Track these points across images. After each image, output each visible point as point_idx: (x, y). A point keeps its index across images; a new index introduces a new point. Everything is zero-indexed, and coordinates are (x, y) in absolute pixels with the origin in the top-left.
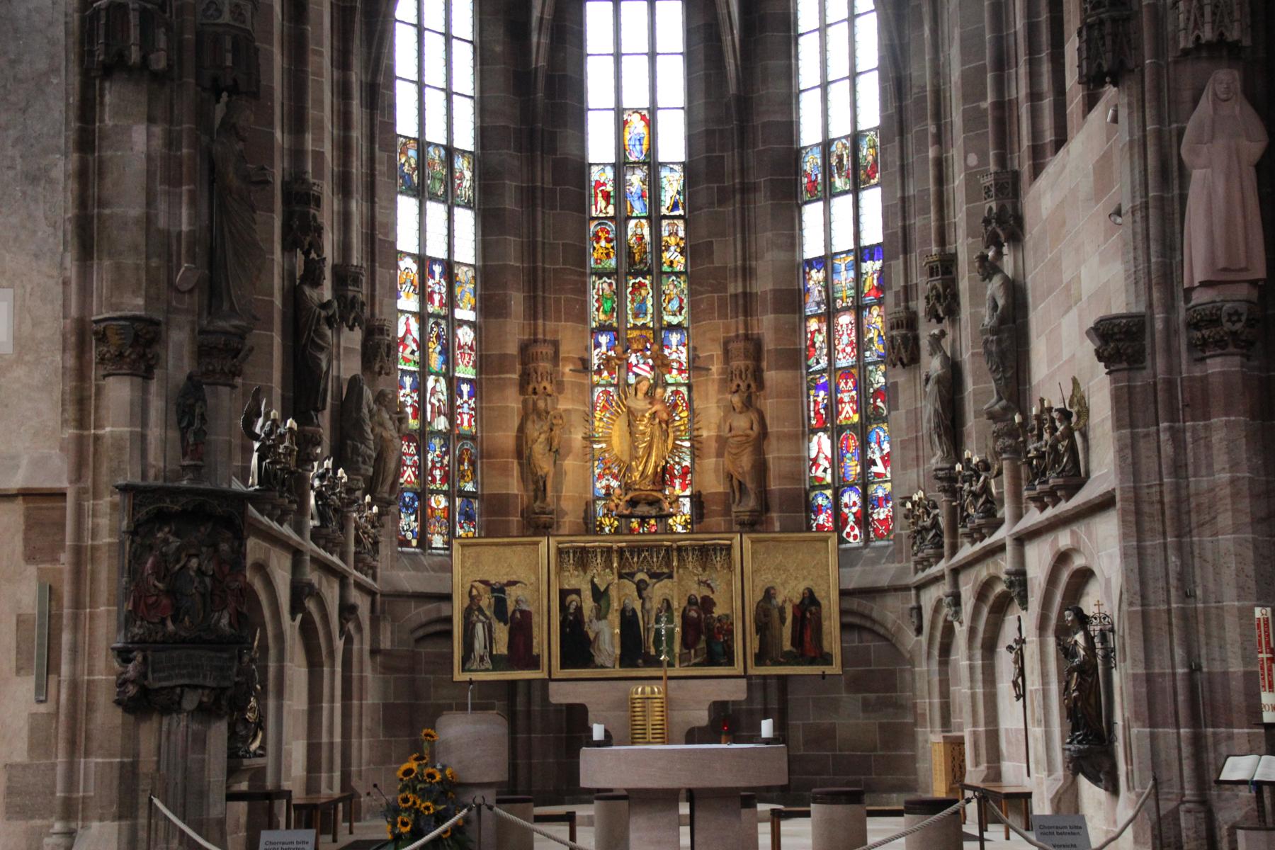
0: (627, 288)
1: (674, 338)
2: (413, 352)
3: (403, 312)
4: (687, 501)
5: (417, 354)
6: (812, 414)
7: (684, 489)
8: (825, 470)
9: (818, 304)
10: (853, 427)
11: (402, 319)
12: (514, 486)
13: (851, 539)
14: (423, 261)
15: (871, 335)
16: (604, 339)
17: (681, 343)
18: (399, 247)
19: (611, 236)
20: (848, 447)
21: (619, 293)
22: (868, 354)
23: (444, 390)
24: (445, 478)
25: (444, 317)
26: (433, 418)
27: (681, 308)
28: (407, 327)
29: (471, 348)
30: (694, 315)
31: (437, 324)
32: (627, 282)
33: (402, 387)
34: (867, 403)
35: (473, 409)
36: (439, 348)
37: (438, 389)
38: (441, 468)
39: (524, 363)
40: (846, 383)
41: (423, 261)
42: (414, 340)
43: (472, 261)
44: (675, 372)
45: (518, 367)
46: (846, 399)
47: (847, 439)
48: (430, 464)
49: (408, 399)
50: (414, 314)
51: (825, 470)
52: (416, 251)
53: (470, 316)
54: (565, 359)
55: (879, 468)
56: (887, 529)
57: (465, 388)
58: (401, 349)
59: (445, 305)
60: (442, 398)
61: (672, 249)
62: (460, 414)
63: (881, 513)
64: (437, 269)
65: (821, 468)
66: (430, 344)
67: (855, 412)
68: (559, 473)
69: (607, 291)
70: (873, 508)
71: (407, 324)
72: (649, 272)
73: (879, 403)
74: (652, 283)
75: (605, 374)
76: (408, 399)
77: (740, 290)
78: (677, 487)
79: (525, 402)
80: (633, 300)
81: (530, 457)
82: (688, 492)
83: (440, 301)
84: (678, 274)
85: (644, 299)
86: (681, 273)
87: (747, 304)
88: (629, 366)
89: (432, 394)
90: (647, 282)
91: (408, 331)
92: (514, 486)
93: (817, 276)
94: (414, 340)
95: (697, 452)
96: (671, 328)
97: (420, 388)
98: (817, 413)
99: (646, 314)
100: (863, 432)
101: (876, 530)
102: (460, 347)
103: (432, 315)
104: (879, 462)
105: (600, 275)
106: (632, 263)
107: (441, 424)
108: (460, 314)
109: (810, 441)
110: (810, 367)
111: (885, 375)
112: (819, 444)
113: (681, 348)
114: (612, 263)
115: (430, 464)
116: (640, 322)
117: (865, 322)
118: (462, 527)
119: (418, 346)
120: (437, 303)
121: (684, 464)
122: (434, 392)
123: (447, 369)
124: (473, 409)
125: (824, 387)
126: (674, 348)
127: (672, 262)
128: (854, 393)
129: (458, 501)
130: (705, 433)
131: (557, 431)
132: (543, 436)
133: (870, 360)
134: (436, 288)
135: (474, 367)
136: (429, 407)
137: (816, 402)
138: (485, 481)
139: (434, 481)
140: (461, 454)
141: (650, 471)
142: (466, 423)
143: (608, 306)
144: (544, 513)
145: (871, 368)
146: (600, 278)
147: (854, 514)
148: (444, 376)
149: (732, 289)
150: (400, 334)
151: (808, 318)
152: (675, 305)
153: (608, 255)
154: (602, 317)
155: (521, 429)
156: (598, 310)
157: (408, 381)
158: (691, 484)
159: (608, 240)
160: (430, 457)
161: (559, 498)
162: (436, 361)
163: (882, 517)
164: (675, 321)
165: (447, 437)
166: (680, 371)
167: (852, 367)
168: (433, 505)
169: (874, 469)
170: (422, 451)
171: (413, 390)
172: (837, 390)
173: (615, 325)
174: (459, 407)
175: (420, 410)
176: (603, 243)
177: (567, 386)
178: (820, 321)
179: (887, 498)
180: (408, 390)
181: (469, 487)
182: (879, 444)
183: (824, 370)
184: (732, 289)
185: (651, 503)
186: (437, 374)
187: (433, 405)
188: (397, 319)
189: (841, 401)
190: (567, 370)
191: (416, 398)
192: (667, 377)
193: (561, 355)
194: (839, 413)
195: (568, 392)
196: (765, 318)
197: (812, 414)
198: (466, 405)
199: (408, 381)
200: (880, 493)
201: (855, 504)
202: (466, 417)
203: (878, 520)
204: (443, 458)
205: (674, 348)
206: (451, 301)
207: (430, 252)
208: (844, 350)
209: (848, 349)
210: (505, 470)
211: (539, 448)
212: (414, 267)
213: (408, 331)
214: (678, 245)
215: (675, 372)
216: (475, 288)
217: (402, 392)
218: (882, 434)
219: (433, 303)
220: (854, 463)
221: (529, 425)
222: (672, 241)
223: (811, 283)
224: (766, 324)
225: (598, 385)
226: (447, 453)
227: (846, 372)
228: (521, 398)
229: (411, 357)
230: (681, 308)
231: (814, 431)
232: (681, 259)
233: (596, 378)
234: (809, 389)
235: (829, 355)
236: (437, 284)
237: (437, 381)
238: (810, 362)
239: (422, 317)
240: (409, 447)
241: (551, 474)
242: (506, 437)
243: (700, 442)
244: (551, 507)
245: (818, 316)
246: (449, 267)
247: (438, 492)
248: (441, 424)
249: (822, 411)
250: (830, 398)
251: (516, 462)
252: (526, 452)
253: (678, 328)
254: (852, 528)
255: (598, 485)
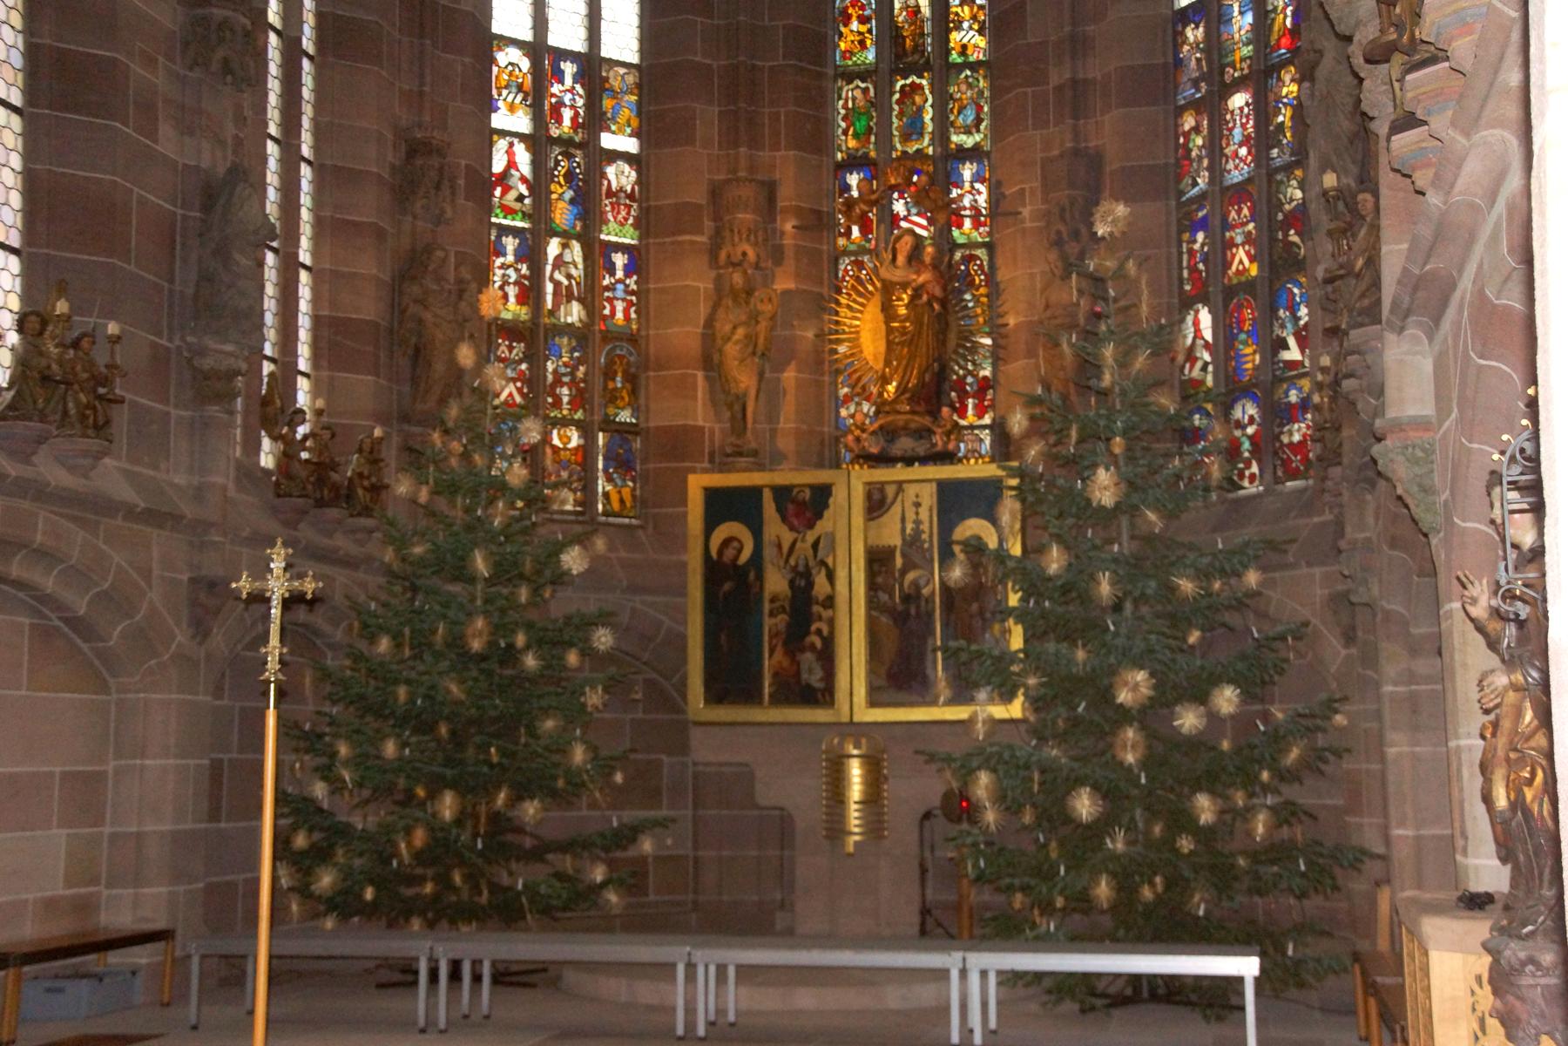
0: (892, 93)
1: (967, 172)
2: (520, 198)
3: (503, 133)
4: (986, 436)
5: (527, 201)
6: (1185, 274)
7: (980, 416)
8: (1204, 368)
9: (1195, 83)
10: (1250, 286)
11: (501, 145)
12: (700, 414)
13: (1246, 483)
14: (538, 49)
15: (1281, 119)
16: (853, 179)
17: (977, 178)
18: (497, 28)
19: (868, 12)
20: (1241, 322)
21: (879, 104)
22: (1275, 152)
23: (579, 260)
24: (578, 400)
25: (580, 146)
26: (556, 305)
27: (979, 121)
28: (511, 158)
29: (631, 196)
30: (997, 133)
31: (569, 156)
32: (892, 84)
33: (501, 253)
34: (1273, 239)
35: (633, 293)
36: (569, 194)
37: (567, 258)
38: (569, 385)
39: (717, 218)
40: (1239, 212)
41: (538, 49)
42: (523, 179)
43: (634, 58)
44: (968, 223)
45: (708, 224)
46: (1239, 240)
47: (1240, 307)
48: (550, 378)
49: (511, 272)
50: (522, 137)
51: (1204, 368)
52: (527, 35)
53: (630, 145)
54: (785, 211)
55: (1293, 354)
56: (1306, 460)
57: (620, 260)
58: (498, 192)
59: (583, 126)
60: (573, 272)
61: (966, 25)
62: (610, 300)
63: (1297, 432)
64: (569, 69)
65: (1199, 365)
66: (553, 187)
67: (1252, 259)
68: (770, 392)
69: (861, 102)
70: (1282, 425)
71: (510, 152)
72: (927, 66)
73: (1294, 237)
74: (932, 85)
75: (856, 231)
76: (511, 272)
77: (1068, 76)
78: (970, 412)
79: (718, 280)
80: (901, 113)
81: (721, 363)
82: (987, 420)
83: (574, 119)
84: (974, 66)
85: (920, 110)
86: (979, 63)
87: (1077, 98)
88: (895, 219)
89: (556, 266)
90: (924, 82)
91: (512, 164)
92: (700, 414)
93: (1194, 34)
94: (523, 179)
95: (1002, 353)
96: (964, 154)
97: (532, 254)
98: (1193, 269)
99: (921, 135)
100: (1268, 293)
101: (1286, 463)
102: (610, 193)
103: (559, 141)
104: (1292, 341)
105: (849, 76)
106: (900, 54)
107: (574, 313)
108: (608, 141)
109: (1183, 320)
110: (1182, 193)
111: (1301, 187)
112: (1196, 323)
113: (977, 185)
114: (870, 56)
115: (550, 378)
116: (912, 148)
117: (1271, 97)
118: (609, 479)
119: (529, 188)
120: (567, 122)
121: (982, 373)
122: (559, 262)
123: (585, 227)
124: (633, 293)
125: (1203, 224)
126: (967, 186)
127: (964, 47)
128: (1251, 226)
129: (601, 438)
130: (1012, 321)
131: (763, 325)
132: (741, 332)
133: (1278, 162)
134: (567, 98)
135: (636, 226)
136: (549, 288)
137: (1191, 252)
138: (653, 406)
139: (557, 403)
140: (610, 362)
141: (914, 381)
142: (620, 315)
143: (861, 125)
144: (740, 454)
145: (1279, 177)
146: (850, 82)
147: (1250, 438)
148: (578, 238)
149: (1055, 79)
150: (498, 165)
151: (1180, 111)
152: (970, 115)
153: (862, 44)
154: (852, 143)
155: (710, 323)
156: (845, 132)
157: (510, 243)
158: (992, 406)
159: (863, 20)
160: (550, 366)
161: (774, 432)
162: (563, 214)
163: (1297, 438)
164: (969, 141)
165: (582, 336)
166: (977, 225)
167: (1249, 180)
168: (556, 441)
169: (1287, 356)
170: (534, 357)
171: (520, 258)
172: (1226, 226)
173: (873, 154)
174: (607, 288)
175: (530, 292)
176: (855, 25)
177: (789, 253)
178: (1198, 113)
179: (1305, 405)
180: (510, 258)
181: (625, 416)
182: (1293, 309)
183: (1203, 196)
184: (1055, 79)
185: (923, 433)
186: (566, 236)
187: (557, 284)
188: (491, 144)
189: (1232, 244)
190: (788, 227)
191: (524, 269)
192: (956, 233)
193: (780, 204)
194: (1228, 265)
195: (790, 263)
196: (1107, 117)
197: (1185, 274)
198: (620, 287)
199: (510, 243)
200: (1293, 397)
201: (1252, 420)
202: (620, 306)
203: (1291, 444)
204: (575, 368)
205: (967, 186)
206: (595, 120)
207: (554, 40)
208: (1236, 154)
209: (1243, 151)
210: (684, 388)
211: (732, 350)
212: (525, 64)
213: (512, 164)
214: (974, 18)
215: (968, 223)
216: (639, 104)
217: (499, 261)
218: (1296, 291)
219: (559, 120)
220: (1248, 350)
221: (721, 313)
222: (966, 12)
223: (1186, 48)
224: (1108, 130)
225: (846, 253)
226: (580, 361)
227: (1239, 193)
228: (713, 274)
229: (517, 206)
230: (979, 121)
231: (1187, 304)
232: (981, 42)
233: (841, 242)
234: (1180, 232)
235: (1210, 169)
236: (567, 90)
237: (565, 246)
238: (1182, 186)
239: (537, 142)
240: (511, 348)
241: (753, 393)
242: (683, 335)
243: (1005, 336)
244: (753, 445)
245: (1196, 106)
246: (592, 66)
247: (564, 423)
248: (574, 313)
249: (1201, 266)
250: (1212, 245)
251: (700, 375)
252: (716, 357)
253: (974, 153)
254: (1248, 466)
255: (843, 412)
